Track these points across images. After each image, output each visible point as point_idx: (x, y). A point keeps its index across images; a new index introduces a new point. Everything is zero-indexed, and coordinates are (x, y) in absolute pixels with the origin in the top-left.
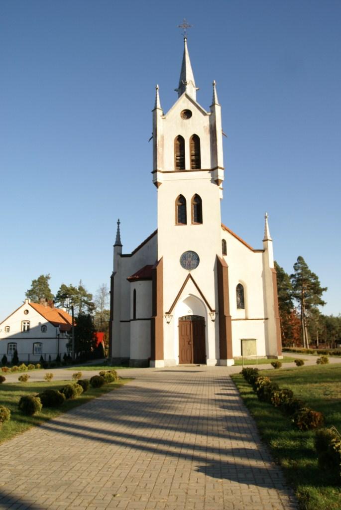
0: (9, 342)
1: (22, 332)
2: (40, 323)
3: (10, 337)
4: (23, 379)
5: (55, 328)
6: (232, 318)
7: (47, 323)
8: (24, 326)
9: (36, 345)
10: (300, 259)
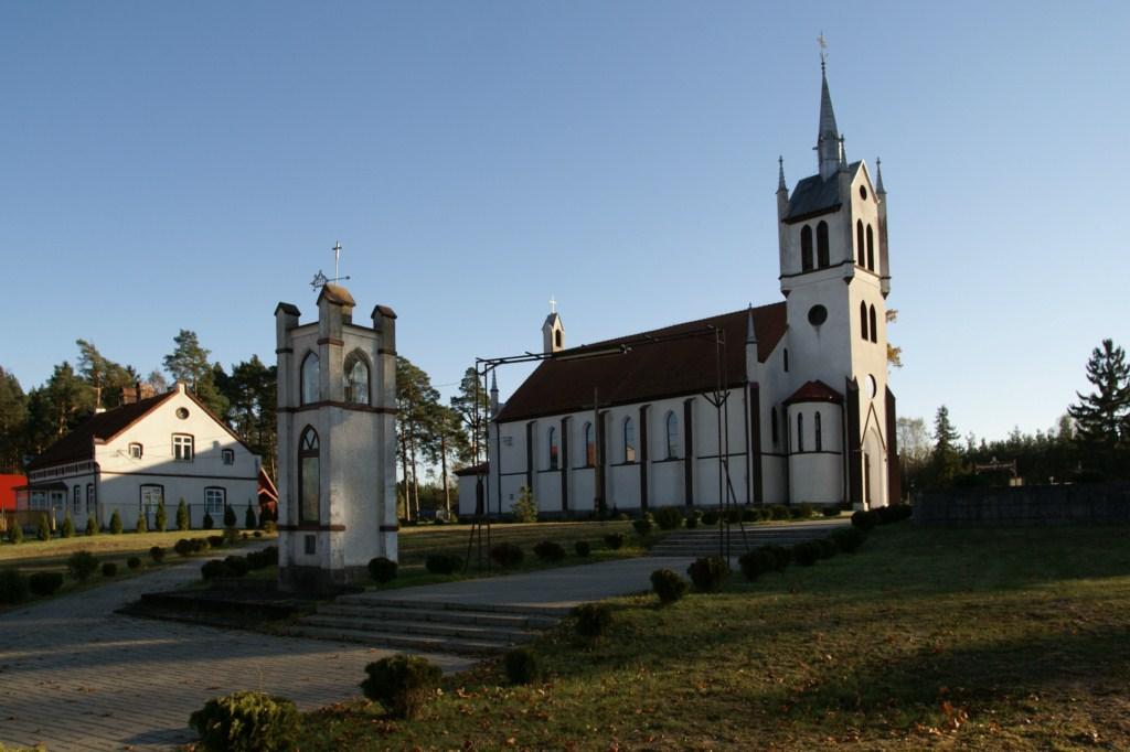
0: (143, 482)
1: (174, 462)
2: (216, 443)
3: (145, 469)
4: (636, 601)
5: (254, 456)
6: (102, 469)
7: (233, 444)
8: (178, 448)
9: (145, 490)
10: (185, 339)
